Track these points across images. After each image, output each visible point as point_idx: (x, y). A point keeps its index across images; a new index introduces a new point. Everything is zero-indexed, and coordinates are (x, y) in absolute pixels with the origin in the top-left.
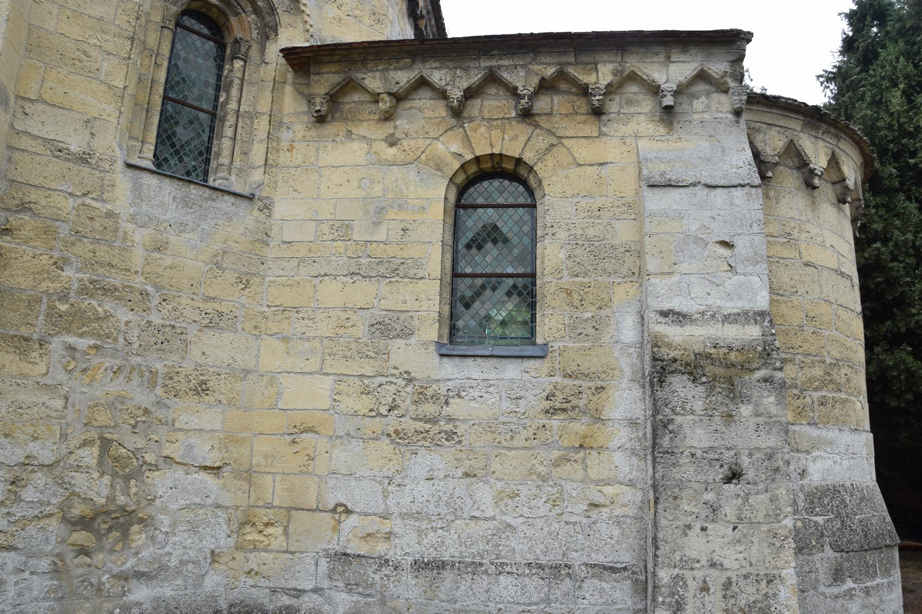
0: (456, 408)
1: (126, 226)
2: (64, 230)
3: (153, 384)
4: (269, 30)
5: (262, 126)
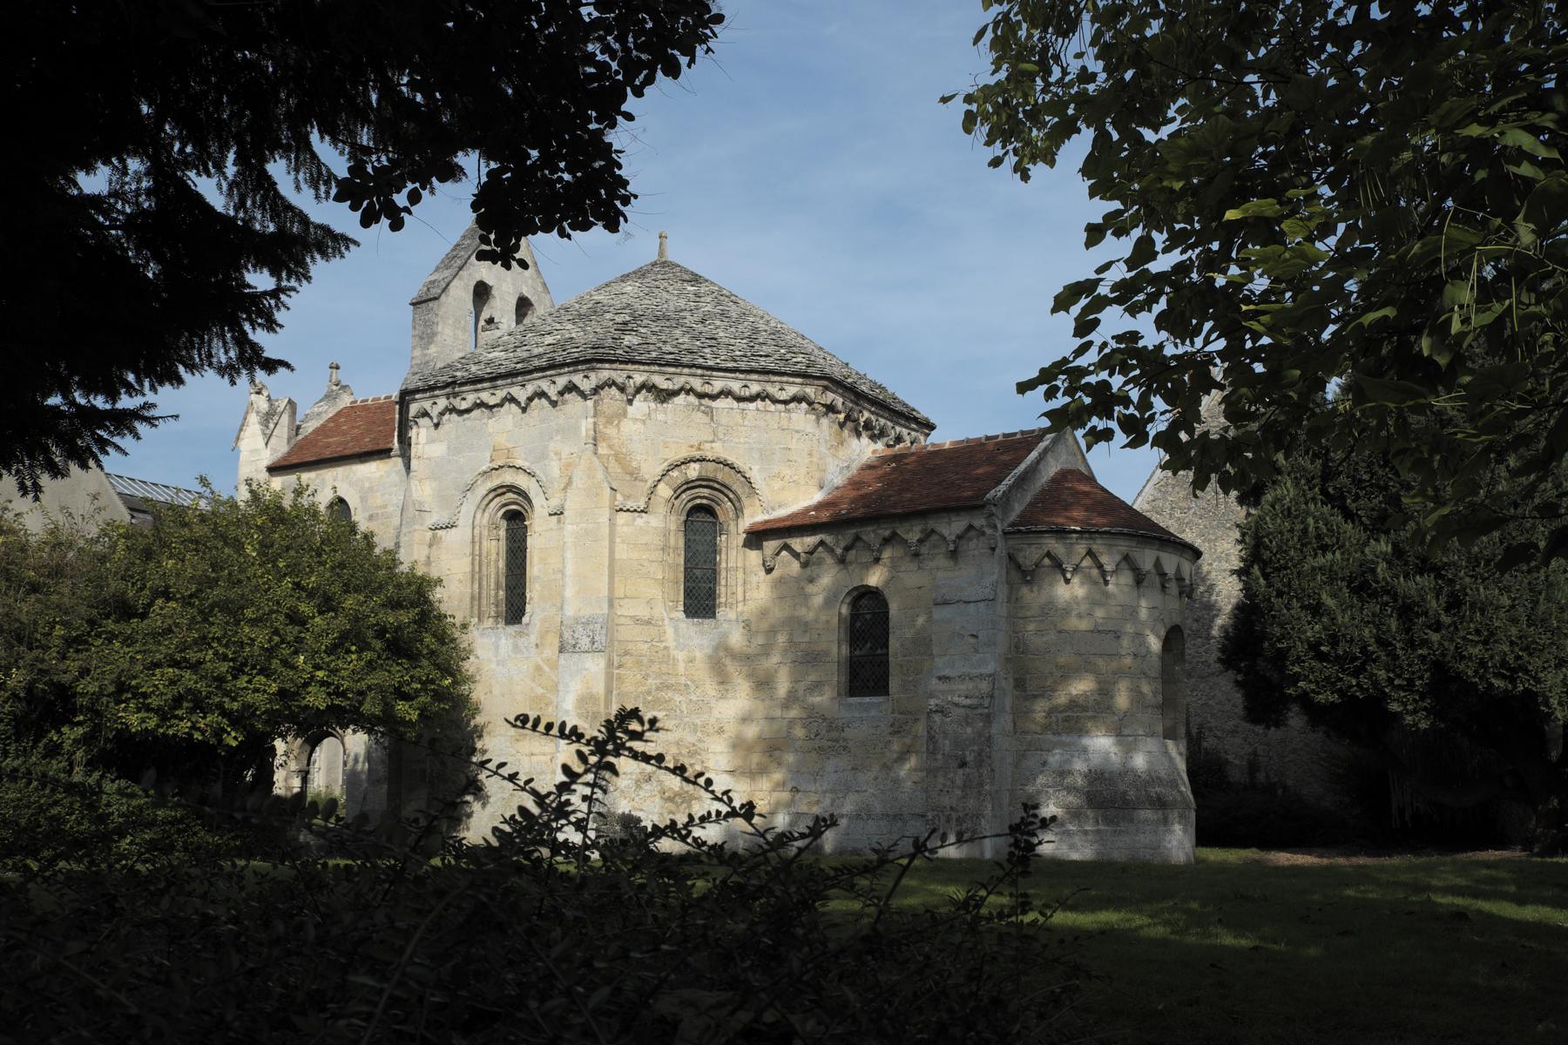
0: (848, 733)
1: (674, 653)
2: (645, 660)
3: (695, 731)
4: (739, 511)
5: (740, 575)
